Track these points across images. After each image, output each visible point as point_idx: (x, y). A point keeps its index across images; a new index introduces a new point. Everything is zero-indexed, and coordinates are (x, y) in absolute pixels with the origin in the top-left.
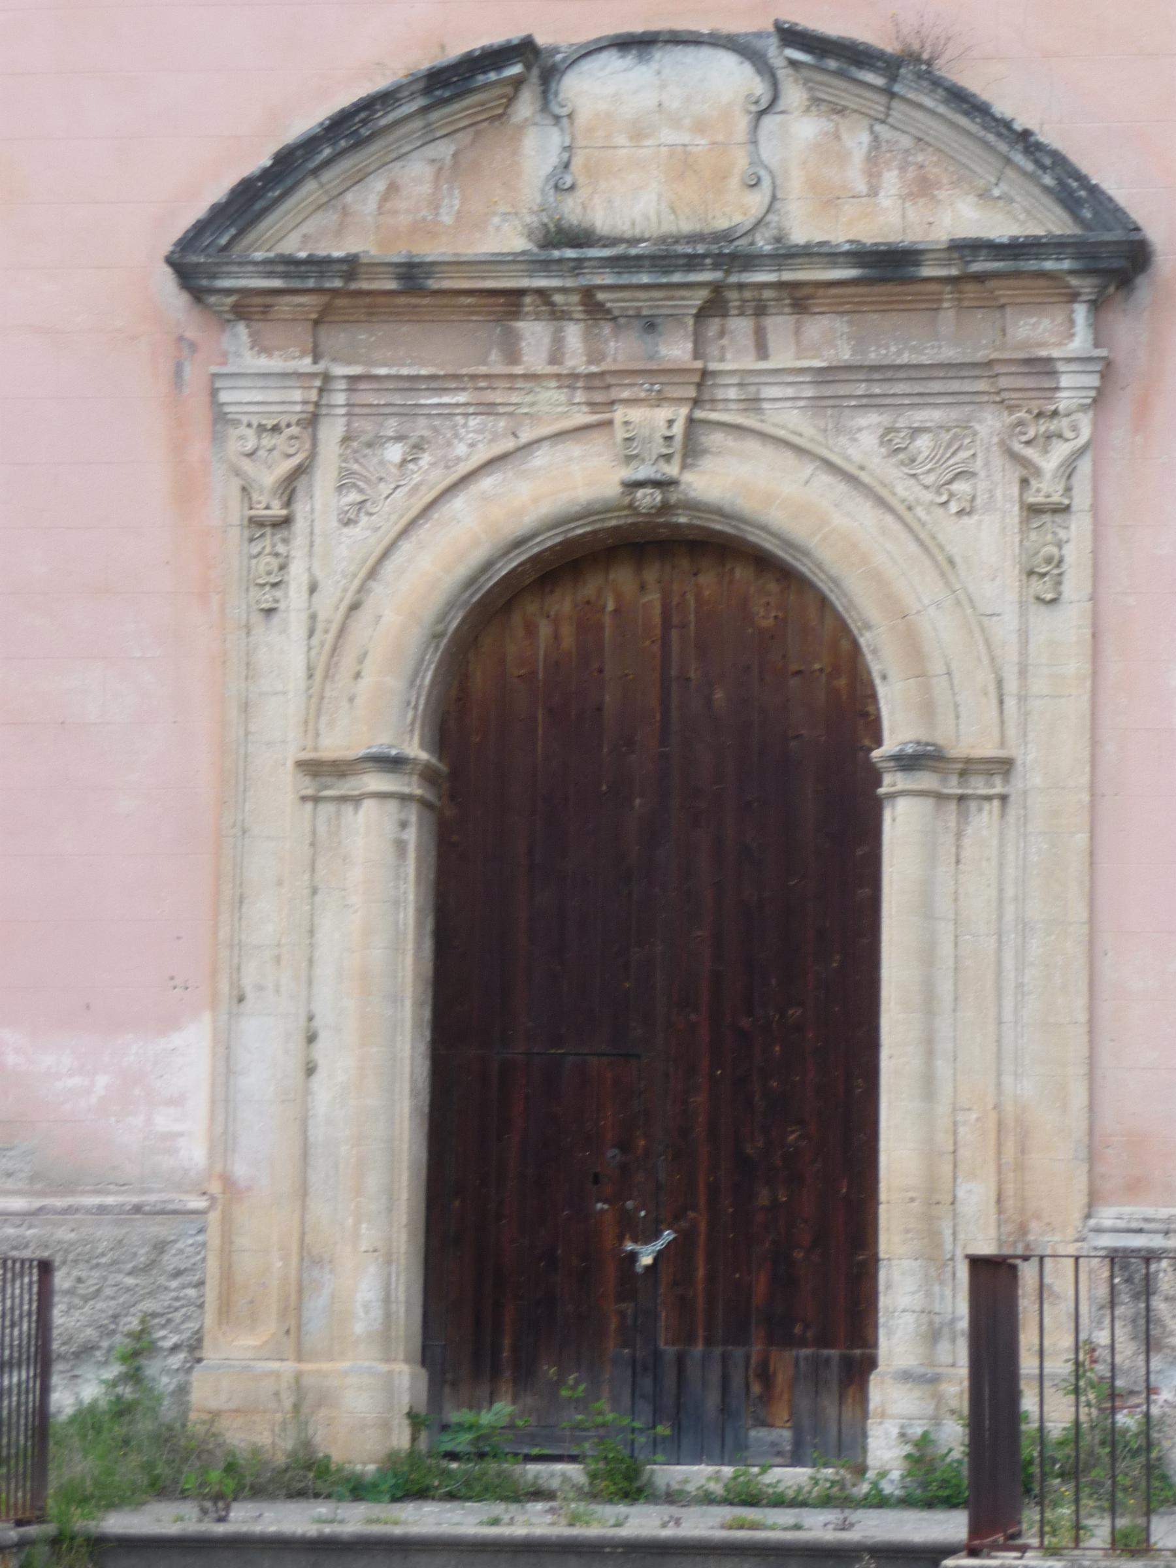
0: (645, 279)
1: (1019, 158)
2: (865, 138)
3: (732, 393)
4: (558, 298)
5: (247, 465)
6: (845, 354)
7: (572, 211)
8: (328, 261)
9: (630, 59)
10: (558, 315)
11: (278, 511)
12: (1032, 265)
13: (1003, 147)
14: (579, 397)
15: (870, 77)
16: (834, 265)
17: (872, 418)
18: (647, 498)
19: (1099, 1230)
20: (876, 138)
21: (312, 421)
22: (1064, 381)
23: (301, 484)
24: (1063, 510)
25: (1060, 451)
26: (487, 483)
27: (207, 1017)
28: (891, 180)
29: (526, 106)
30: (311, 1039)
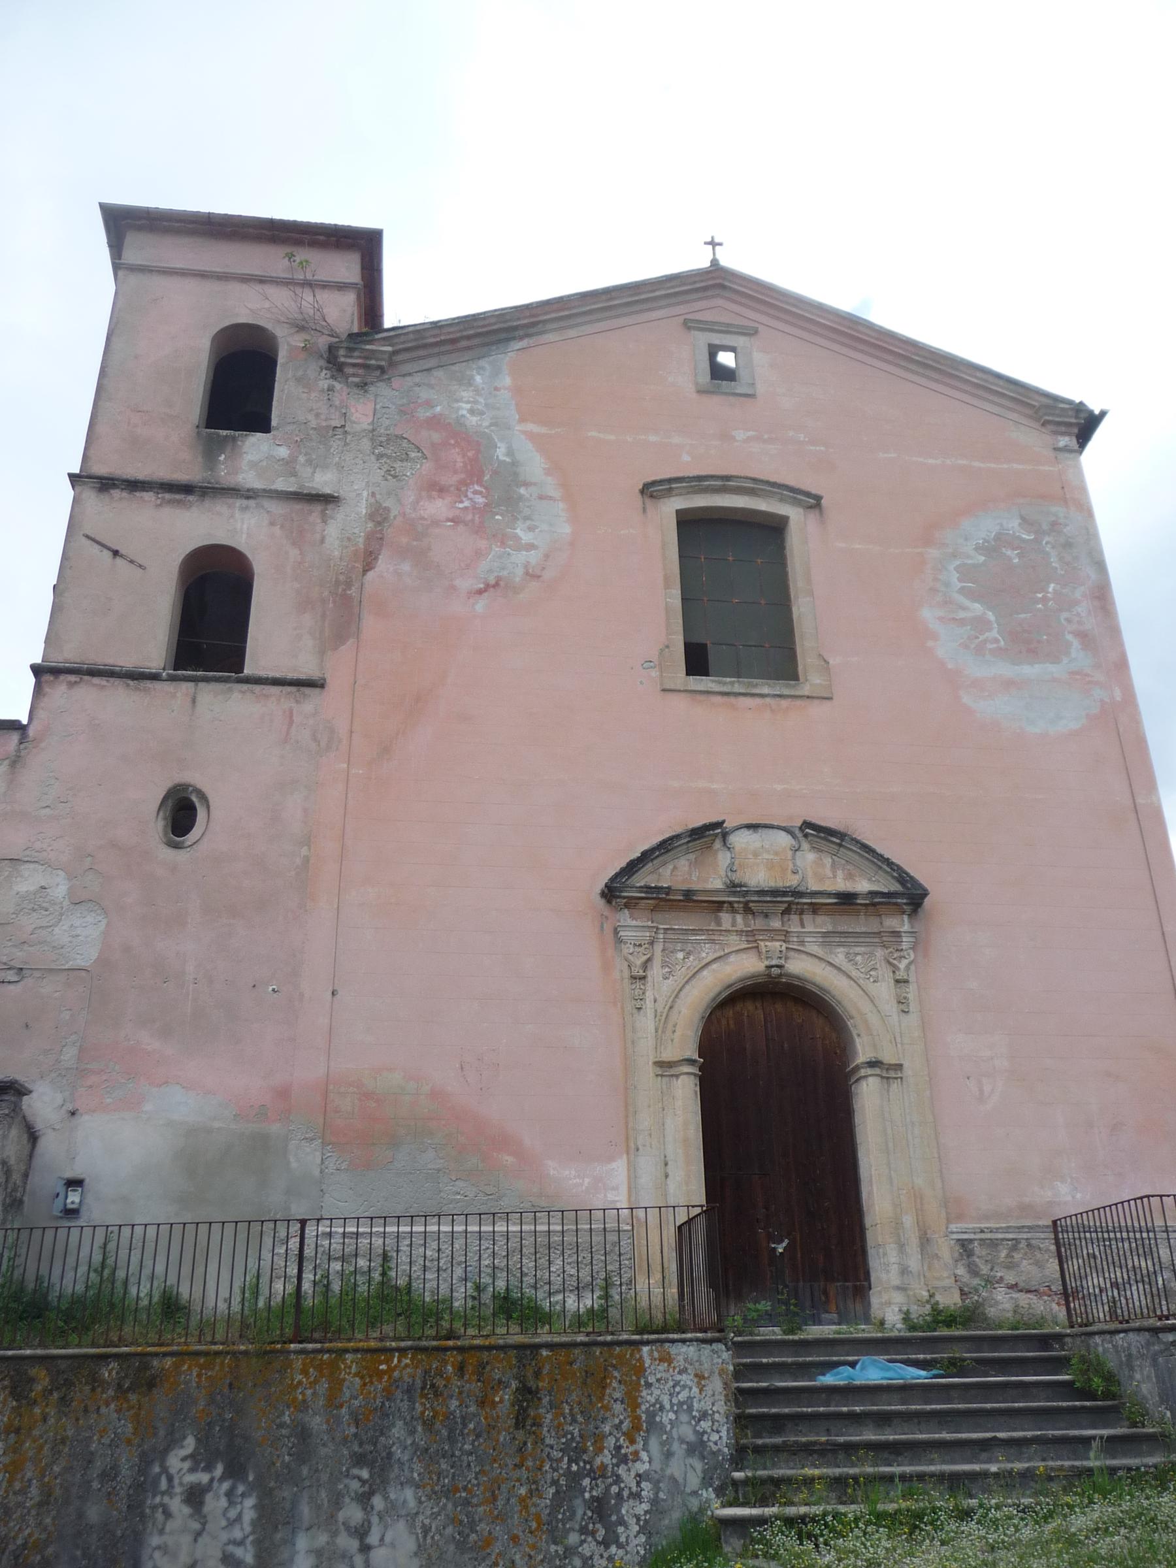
0: (768, 899)
1: (885, 867)
2: (830, 860)
3: (795, 939)
4: (736, 905)
5: (630, 957)
6: (830, 928)
7: (736, 877)
8: (662, 888)
9: (751, 831)
10: (734, 911)
11: (641, 973)
12: (894, 900)
13: (880, 863)
14: (744, 938)
15: (834, 839)
16: (830, 898)
17: (841, 949)
18: (775, 971)
19: (952, 1233)
20: (833, 860)
21: (652, 943)
22: (904, 939)
23: (649, 965)
24: (906, 981)
25: (905, 962)
26: (714, 966)
27: (625, 1156)
28: (840, 873)
29: (718, 844)
30: (666, 1164)
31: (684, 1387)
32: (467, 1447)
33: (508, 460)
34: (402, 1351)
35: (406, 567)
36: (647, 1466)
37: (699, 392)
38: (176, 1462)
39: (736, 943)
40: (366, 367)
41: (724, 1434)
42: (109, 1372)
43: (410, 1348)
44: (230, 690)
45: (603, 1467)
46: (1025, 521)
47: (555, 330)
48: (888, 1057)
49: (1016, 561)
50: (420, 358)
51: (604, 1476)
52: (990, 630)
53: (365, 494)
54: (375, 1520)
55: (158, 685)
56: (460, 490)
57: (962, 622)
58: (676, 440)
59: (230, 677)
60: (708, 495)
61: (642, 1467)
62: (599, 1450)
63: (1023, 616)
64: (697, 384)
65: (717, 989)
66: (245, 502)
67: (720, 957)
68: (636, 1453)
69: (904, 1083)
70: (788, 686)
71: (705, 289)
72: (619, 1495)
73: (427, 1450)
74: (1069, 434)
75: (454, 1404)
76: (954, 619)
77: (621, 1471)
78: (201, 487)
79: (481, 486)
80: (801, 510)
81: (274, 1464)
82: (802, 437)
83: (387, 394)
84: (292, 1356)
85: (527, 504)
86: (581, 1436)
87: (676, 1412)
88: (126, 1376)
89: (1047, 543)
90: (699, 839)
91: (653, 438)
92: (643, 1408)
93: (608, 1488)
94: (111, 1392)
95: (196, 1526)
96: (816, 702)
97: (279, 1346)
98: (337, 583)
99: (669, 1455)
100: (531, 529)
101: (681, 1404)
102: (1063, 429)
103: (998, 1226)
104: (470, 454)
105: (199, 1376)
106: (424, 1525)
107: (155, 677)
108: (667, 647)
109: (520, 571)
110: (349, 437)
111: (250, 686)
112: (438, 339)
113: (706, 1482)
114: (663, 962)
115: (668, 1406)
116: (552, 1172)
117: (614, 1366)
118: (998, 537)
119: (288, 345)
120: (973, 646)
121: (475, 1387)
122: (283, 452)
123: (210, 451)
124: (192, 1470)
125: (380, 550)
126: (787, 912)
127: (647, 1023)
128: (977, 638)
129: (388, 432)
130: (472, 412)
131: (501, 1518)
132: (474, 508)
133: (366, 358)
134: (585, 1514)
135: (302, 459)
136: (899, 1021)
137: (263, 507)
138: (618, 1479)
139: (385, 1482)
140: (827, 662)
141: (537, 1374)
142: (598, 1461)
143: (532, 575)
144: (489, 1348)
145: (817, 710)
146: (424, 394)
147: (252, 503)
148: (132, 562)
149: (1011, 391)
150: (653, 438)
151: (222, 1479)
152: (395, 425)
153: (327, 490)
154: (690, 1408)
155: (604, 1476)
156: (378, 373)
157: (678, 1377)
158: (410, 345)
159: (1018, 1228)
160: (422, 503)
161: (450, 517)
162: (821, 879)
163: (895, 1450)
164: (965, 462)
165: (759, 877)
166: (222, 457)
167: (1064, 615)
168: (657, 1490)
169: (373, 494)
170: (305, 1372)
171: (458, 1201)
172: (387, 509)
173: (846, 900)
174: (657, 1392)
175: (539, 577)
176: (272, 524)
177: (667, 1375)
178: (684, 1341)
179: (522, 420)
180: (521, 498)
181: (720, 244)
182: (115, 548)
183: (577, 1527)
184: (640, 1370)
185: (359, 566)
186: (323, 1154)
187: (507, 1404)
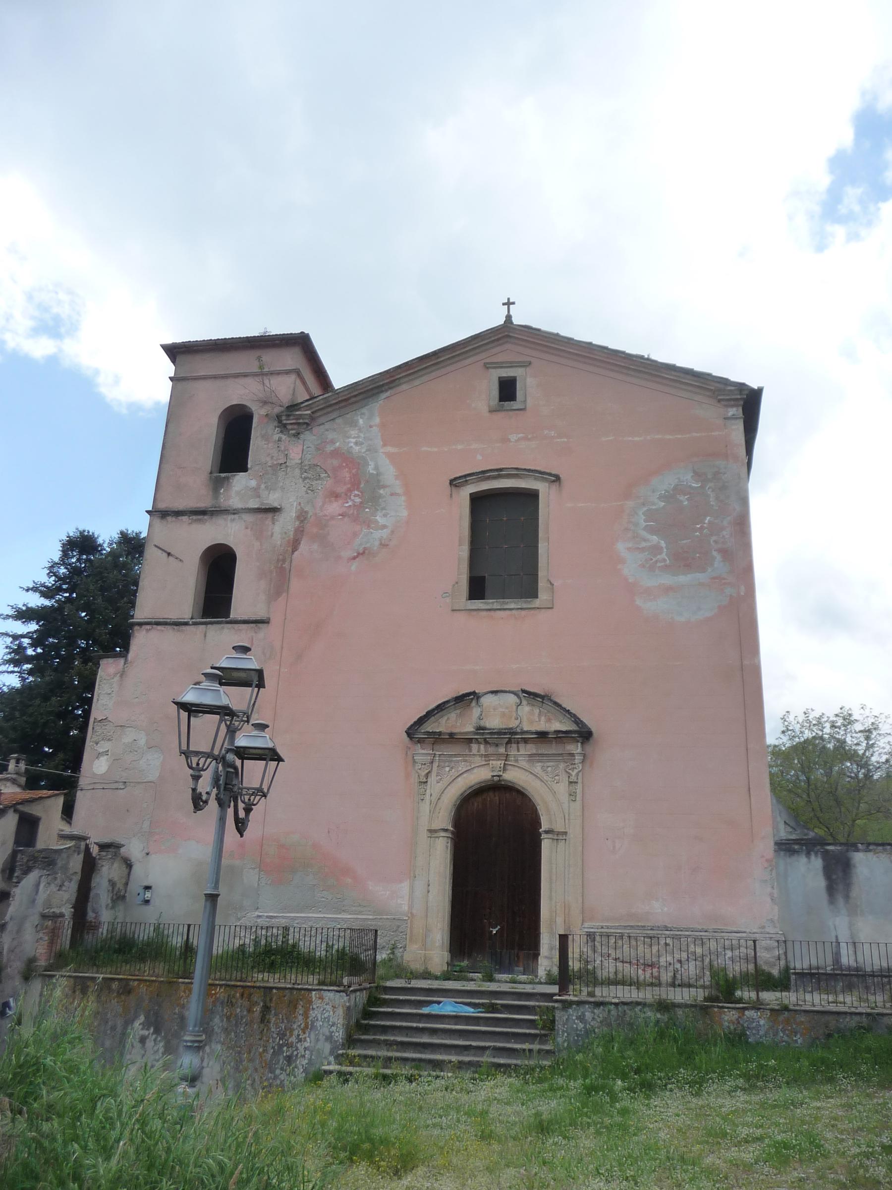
0: (496, 736)
1: (567, 715)
2: (538, 711)
3: (513, 759)
4: (479, 740)
5: (419, 770)
6: (534, 752)
7: (482, 723)
8: (436, 732)
9: (493, 695)
10: (479, 743)
11: (425, 780)
12: (570, 735)
13: (564, 713)
14: (483, 759)
15: (539, 699)
16: (532, 734)
17: (540, 764)
18: (496, 779)
19: (584, 928)
20: (540, 711)
21: (432, 763)
22: (577, 757)
23: (429, 775)
24: (576, 783)
25: (576, 771)
26: (465, 775)
27: (408, 881)
28: (543, 718)
29: (474, 704)
30: (429, 885)
31: (327, 1011)
32: (242, 1029)
33: (375, 473)
34: (221, 986)
35: (315, 547)
36: (308, 1044)
37: (490, 411)
38: (137, 1024)
39: (478, 761)
40: (298, 424)
41: (341, 1033)
42: (115, 985)
43: (224, 985)
44: (223, 628)
45: (292, 1043)
46: (697, 475)
47: (405, 383)
48: (559, 828)
49: (686, 503)
50: (328, 413)
51: (292, 1047)
52: (660, 553)
53: (295, 503)
54: (206, 1056)
55: (188, 628)
56: (348, 494)
57: (643, 550)
58: (474, 446)
59: (222, 621)
60: (489, 482)
61: (307, 1044)
62: (291, 1035)
63: (685, 542)
64: (489, 406)
65: (463, 789)
66: (233, 516)
67: (468, 770)
68: (305, 1038)
69: (567, 842)
70: (525, 602)
71: (498, 340)
72: (297, 1055)
73: (227, 1029)
74: (737, 406)
75: (238, 1010)
76: (638, 548)
77: (299, 1045)
78: (210, 511)
79: (359, 491)
80: (547, 484)
81: (171, 1029)
82: (553, 434)
83: (310, 438)
84: (180, 985)
85: (384, 500)
86: (285, 1029)
87: (323, 1022)
88: (121, 988)
89: (708, 489)
90: (460, 702)
91: (460, 447)
92: (310, 1019)
93: (293, 1053)
94: (115, 994)
95: (143, 1052)
96: (543, 610)
97: (175, 980)
98: (278, 560)
99: (318, 1040)
100: (385, 515)
101: (325, 1018)
102: (732, 403)
103: (613, 925)
104: (354, 471)
105: (146, 990)
106: (223, 1061)
107: (186, 624)
108: (457, 583)
109: (377, 543)
110: (289, 469)
111: (233, 625)
112: (337, 401)
113: (331, 1053)
114: (438, 773)
115: (320, 1019)
116: (370, 888)
117: (301, 999)
118: (675, 488)
119: (258, 412)
120: (648, 566)
121: (246, 1003)
122: (253, 483)
123: (217, 484)
124: (142, 1029)
125: (302, 538)
126: (509, 742)
127: (425, 807)
128: (652, 559)
129: (310, 463)
130: (356, 443)
131: (251, 1060)
132: (355, 505)
133: (297, 419)
134: (283, 1062)
135: (263, 486)
136: (569, 807)
137: (242, 518)
138: (297, 1049)
139: (211, 1041)
140: (552, 584)
141: (271, 1000)
142: (290, 1040)
143: (383, 545)
144: (253, 987)
145: (543, 615)
146: (330, 436)
147: (236, 516)
148: (177, 558)
149: (696, 381)
150: (460, 447)
151: (153, 1034)
152: (314, 458)
153: (276, 505)
154: (329, 1021)
155: (292, 1047)
156: (305, 426)
157: (325, 1007)
158: (322, 407)
159: (625, 926)
160: (326, 506)
161: (341, 513)
162: (531, 722)
163: (404, 1046)
164: (660, 437)
165: (494, 722)
166: (222, 491)
167: (714, 538)
168: (311, 1055)
169: (300, 504)
170: (185, 992)
171: (323, 901)
172: (306, 512)
173: (542, 736)
174: (316, 1012)
175: (388, 545)
176: (247, 528)
177: (320, 1005)
178: (329, 990)
179: (385, 445)
180: (380, 496)
181: (513, 303)
182: (169, 551)
183: (280, 1067)
184: (310, 1002)
185: (290, 549)
186: (259, 876)
187: (258, 1012)
